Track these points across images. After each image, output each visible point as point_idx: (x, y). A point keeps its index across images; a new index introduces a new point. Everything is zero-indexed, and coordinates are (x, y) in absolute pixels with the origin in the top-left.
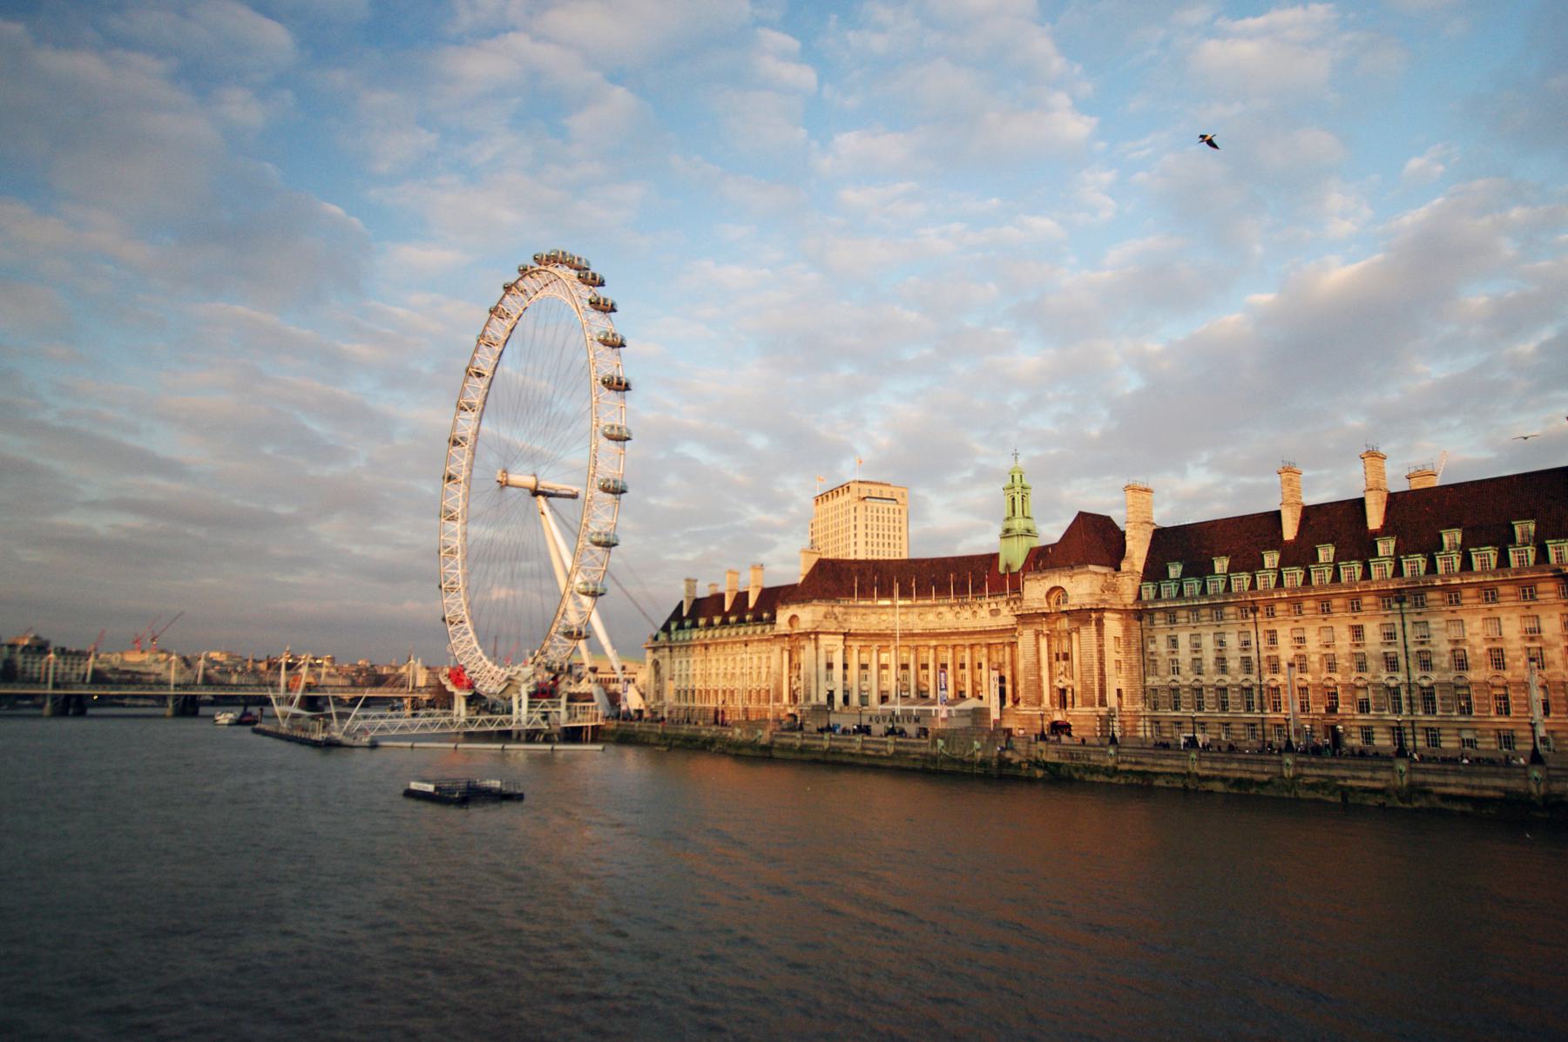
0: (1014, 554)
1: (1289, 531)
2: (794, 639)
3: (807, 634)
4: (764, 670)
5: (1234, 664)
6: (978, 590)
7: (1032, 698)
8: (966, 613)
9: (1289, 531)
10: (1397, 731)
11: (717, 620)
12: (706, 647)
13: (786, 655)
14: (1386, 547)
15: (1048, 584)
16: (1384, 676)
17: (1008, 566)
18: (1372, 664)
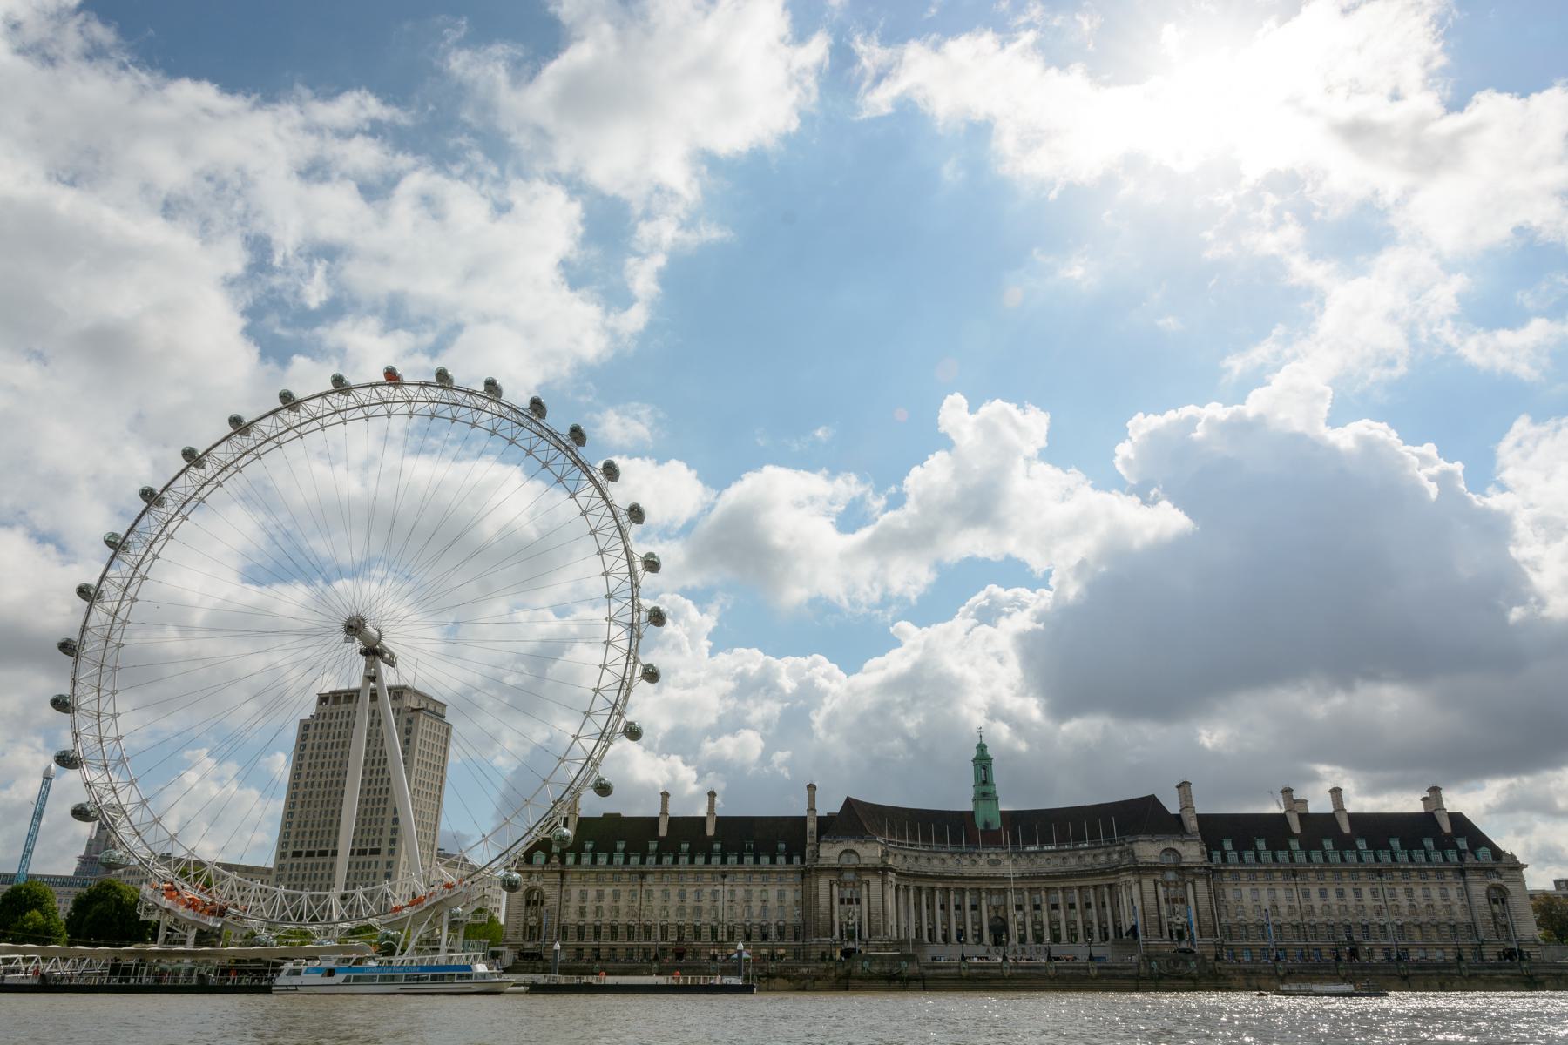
0: (988, 816)
1: (1296, 829)
2: (851, 876)
3: (875, 870)
4: (756, 905)
5: (1283, 910)
6: (972, 840)
7: (1156, 932)
8: (965, 862)
9: (1296, 829)
10: (1387, 951)
11: (653, 846)
12: (643, 875)
13: (835, 888)
14: (1362, 844)
15: (1162, 846)
16: (1376, 919)
17: (987, 825)
18: (1368, 911)
